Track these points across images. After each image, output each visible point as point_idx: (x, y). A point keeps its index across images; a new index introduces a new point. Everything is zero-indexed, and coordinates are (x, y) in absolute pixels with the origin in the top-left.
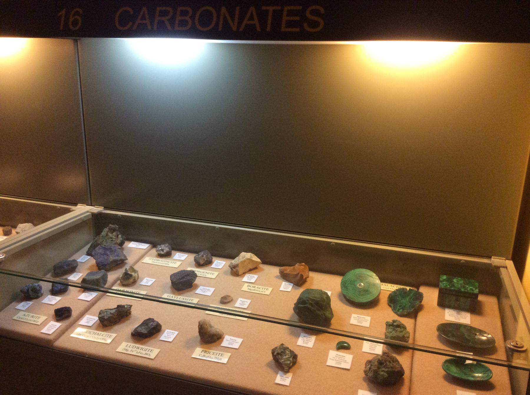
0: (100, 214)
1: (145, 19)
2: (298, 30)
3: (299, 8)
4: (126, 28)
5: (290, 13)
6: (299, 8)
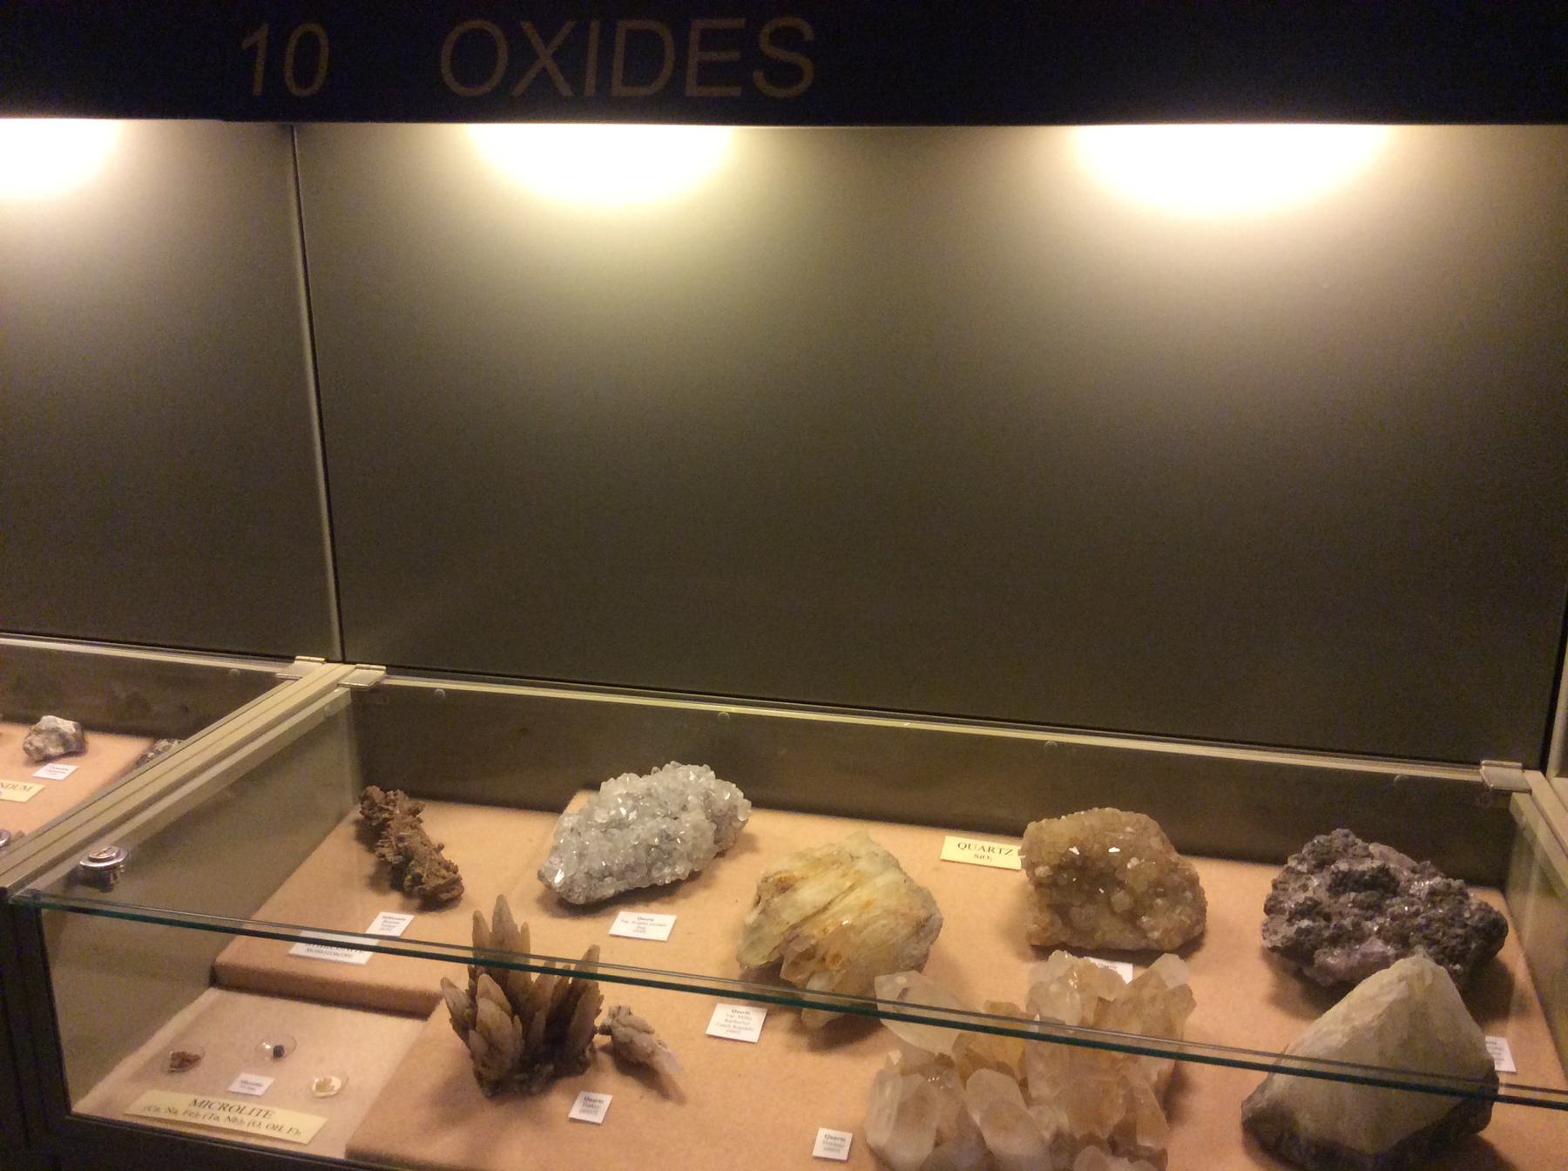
0: (377, 689)
2: (736, 91)
3: (739, 23)
4: (486, 88)
6: (739, 23)
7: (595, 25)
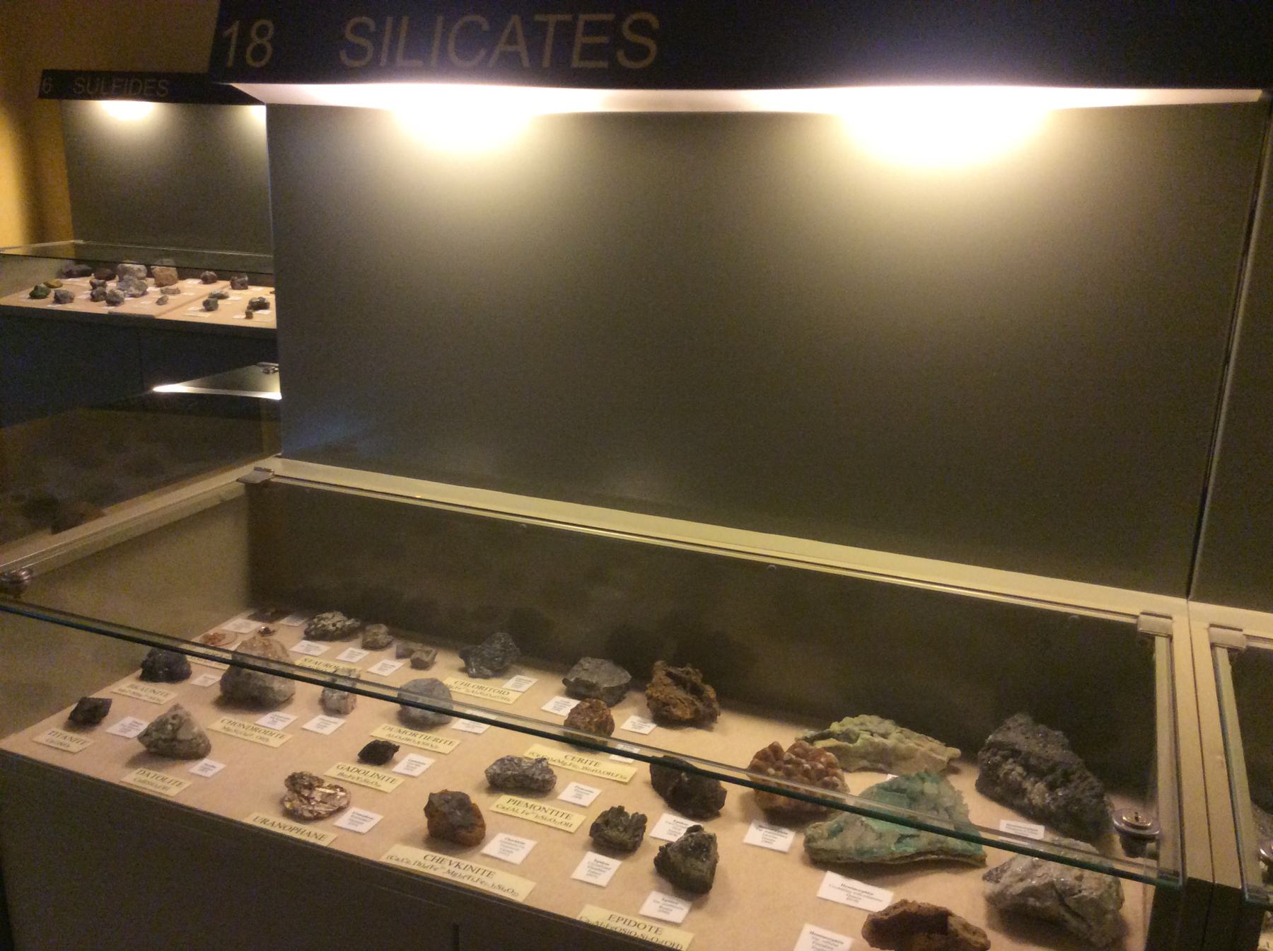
1: (516, 43)
5: (591, 28)
7: (390, 20)
